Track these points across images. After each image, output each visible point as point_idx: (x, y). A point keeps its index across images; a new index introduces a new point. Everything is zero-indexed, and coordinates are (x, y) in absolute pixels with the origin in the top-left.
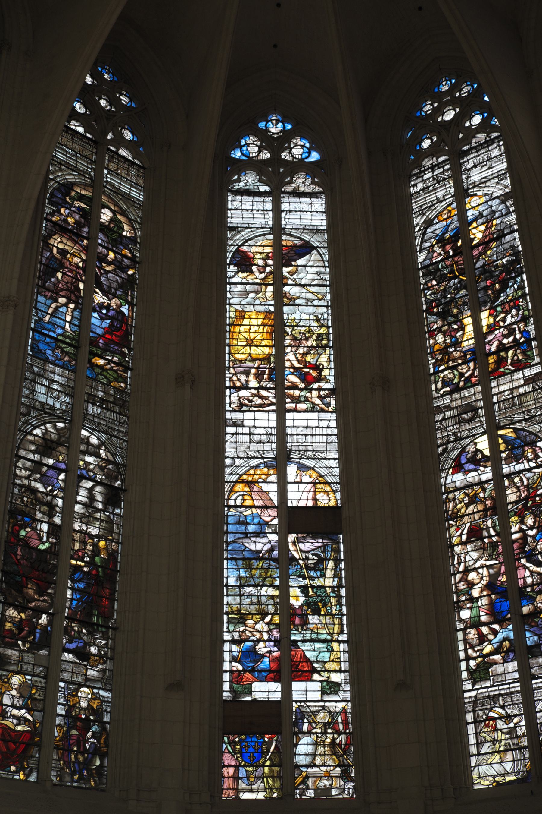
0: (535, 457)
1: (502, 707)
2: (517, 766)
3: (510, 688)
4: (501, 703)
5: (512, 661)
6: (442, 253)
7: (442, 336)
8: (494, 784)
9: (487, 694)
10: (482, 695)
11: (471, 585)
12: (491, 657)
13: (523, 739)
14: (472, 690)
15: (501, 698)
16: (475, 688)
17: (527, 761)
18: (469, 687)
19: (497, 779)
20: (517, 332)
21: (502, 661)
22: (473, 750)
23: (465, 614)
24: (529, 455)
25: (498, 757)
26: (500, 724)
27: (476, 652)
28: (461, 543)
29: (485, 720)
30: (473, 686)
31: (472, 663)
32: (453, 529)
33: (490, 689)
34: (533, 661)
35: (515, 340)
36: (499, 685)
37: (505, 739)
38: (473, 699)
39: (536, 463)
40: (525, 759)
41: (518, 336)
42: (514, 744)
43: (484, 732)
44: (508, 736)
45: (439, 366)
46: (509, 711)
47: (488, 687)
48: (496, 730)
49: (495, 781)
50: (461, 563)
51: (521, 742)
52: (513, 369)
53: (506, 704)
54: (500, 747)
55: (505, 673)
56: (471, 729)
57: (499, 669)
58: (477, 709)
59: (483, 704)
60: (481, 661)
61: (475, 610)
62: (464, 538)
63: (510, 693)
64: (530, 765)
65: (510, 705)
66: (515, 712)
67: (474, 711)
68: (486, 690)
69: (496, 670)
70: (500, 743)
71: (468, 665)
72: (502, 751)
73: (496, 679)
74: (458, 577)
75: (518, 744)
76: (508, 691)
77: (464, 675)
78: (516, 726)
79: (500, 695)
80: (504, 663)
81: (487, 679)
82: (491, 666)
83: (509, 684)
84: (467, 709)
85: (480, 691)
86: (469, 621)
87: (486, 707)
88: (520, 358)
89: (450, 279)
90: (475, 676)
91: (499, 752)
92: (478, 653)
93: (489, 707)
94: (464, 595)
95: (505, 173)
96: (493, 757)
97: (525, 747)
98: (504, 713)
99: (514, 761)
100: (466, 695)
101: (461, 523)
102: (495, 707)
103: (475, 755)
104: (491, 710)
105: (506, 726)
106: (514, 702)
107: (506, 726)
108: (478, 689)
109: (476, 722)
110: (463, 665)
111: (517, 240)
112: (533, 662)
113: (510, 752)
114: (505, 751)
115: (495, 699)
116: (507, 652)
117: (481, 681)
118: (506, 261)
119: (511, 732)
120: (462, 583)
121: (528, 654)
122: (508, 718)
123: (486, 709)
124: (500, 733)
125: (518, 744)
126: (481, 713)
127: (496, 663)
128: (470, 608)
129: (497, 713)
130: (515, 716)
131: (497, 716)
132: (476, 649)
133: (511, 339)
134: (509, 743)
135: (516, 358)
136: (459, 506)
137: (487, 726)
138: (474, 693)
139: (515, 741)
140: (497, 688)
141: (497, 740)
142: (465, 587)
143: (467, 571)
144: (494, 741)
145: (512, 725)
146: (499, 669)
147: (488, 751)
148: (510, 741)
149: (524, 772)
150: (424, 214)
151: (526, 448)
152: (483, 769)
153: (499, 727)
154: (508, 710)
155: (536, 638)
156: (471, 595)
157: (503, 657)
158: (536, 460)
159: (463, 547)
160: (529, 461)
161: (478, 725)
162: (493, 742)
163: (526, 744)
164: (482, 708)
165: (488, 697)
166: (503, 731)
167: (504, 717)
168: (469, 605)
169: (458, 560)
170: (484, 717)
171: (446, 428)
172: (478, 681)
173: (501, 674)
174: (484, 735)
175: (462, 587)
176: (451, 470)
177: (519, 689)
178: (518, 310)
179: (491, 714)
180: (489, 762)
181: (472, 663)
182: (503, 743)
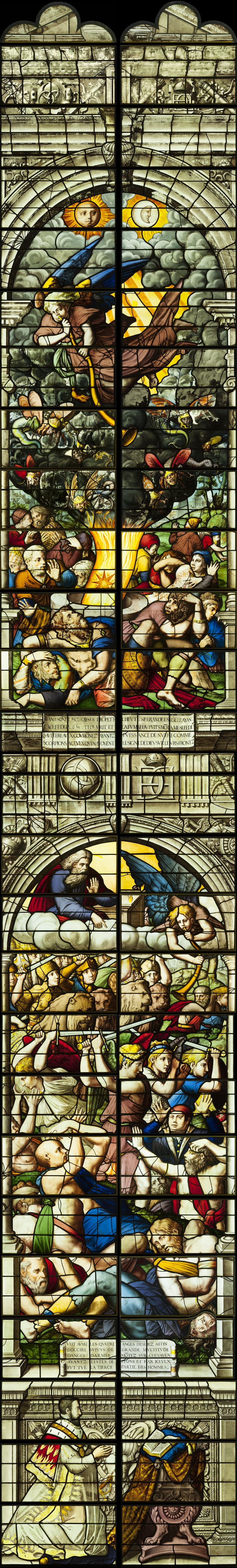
0: (191, 926)
6: (65, 323)
7: (39, 554)
8: (43, 1561)
9: (48, 1393)
10: (38, 1393)
11: (43, 1166)
14: (21, 1379)
20: (197, 617)
23: (24, 1225)
24: (181, 918)
28: (32, 1072)
29: (37, 1442)
30: (24, 1370)
32: (17, 1036)
35: (190, 629)
39: (192, 941)
41: (198, 628)
45: (26, 633)
48: (56, 1462)
49: (45, 1555)
50: (26, 1114)
52: (175, 702)
58: (27, 1416)
61: (45, 1220)
62: (40, 1062)
68: (48, 1384)
71: (17, 1331)
74: (19, 1142)
85: (35, 1384)
86: (29, 1239)
88: (195, 682)
89: (76, 409)
92: (42, 1309)
94: (25, 1185)
95: (228, 168)
101: (37, 1027)
104: (53, 1423)
108: (32, 1380)
111: (231, 373)
117: (40, 1365)
118: (198, 419)
120: (25, 1158)
123: (43, 1420)
128: (36, 1215)
132: (39, 1299)
133: (181, 628)
135: (185, 679)
136: (36, 989)
142: (30, 1167)
143: (37, 1136)
144: (53, 1482)
150: (32, 184)
151: (177, 901)
152: (29, 1532)
156: (40, 1188)
158: (193, 934)
159: (35, 1082)
160: (178, 932)
161: (24, 1448)
168: (33, 1208)
169: (21, 1107)
171: (26, 795)
175: (23, 1168)
176: (28, 899)
178: (207, 561)
180: (38, 1520)
181: (27, 1328)
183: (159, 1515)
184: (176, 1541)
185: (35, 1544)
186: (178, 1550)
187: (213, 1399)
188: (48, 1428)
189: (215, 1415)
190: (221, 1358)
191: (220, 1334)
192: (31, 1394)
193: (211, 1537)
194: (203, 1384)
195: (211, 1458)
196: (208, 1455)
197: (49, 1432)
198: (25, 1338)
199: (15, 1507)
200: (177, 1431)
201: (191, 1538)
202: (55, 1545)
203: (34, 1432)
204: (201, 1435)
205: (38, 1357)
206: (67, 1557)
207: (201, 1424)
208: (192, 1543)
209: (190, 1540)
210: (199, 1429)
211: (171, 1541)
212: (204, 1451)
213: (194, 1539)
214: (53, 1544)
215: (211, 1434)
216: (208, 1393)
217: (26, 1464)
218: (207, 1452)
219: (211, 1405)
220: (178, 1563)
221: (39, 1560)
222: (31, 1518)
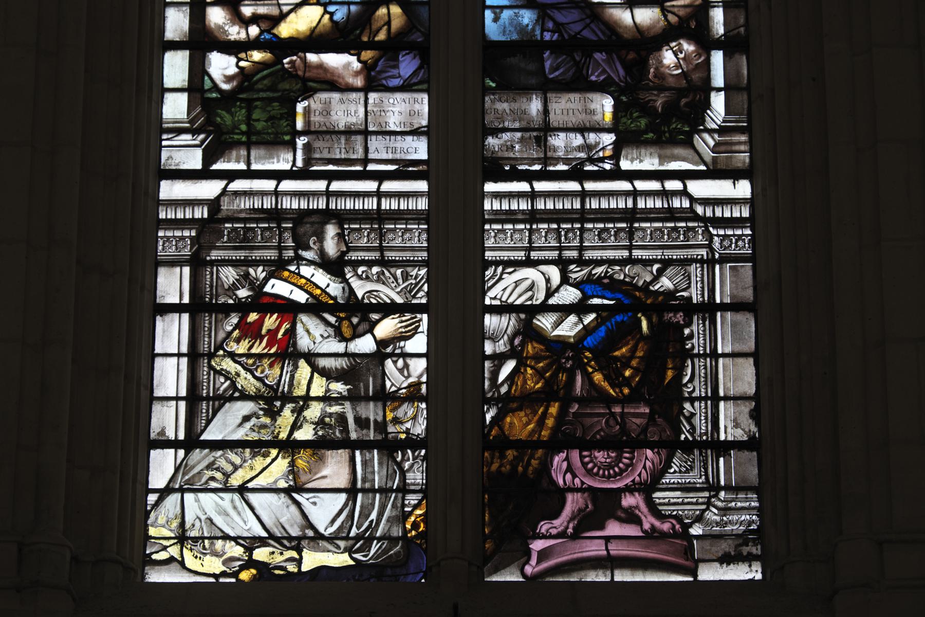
1: (335, 267)
2: (365, 515)
3: (379, 194)
4: (331, 247)
5: (406, 87)
8: (245, 576)
9: (268, 203)
10: (245, 204)
12: (312, 57)
13: (406, 410)
15: (331, 231)
16: (218, 166)
17: (412, 499)
18: (194, 160)
19: (261, 554)
21: (359, 82)
22: (168, 419)
25: (282, 465)
26: (312, 334)
27: (245, 22)
29: (242, 308)
30: (210, 156)
31: (221, 66)
33: (287, 185)
34: (504, 106)
36: (331, 177)
37: (326, 399)
38: (201, 213)
40: (404, 489)
42: (362, 423)
43: (232, 356)
44: (338, 387)
46: (360, 289)
47: (278, 176)
48: (288, 352)
49: (250, 563)
51: (396, 421)
53: (354, 256)
54: (295, 427)
55: (366, 133)
56: (171, 334)
57: (346, 111)
58: (215, 255)
59: (244, 240)
60: (262, 65)
63: (380, 217)
64: (426, 517)
65: (370, 264)
66: (389, 294)
67: (198, 263)
68: (269, 185)
69: (327, 112)
70: (299, 411)
72: (305, 444)
73: (322, 149)
75: (381, 427)
76: (371, 204)
77: (175, 107)
78: (386, 349)
79: (328, 215)
80: (366, 89)
81: (282, 139)
82: (307, 93)
83: (381, 177)
84: (164, 250)
85: (238, 185)
87: (257, 254)
90: (225, 118)
91: (289, 447)
92: (254, 30)
93: (271, 254)
96: (259, 462)
97: (412, 443)
98: (335, 289)
99: (352, 491)
100: (169, 190)
102: (298, 259)
103: (174, 444)
104: (277, 268)
105: (340, 347)
106: (390, 255)
107: (340, 347)
109: (198, 307)
110: (175, 69)
112: (499, 106)
113: (343, 454)
114: (320, 445)
115: (307, 228)
116: (392, 48)
117: (248, 146)
119: (361, 375)
121: (486, 73)
122: (354, 314)
123: (255, 263)
124: (304, 370)
125: (381, 427)
126: (229, 275)
127: (331, 83)
129: (308, 285)
130: (388, 309)
131: (300, 297)
132: (247, 11)
134: (341, 419)
137: (251, 332)
138: (210, 189)
139: (371, 411)
140: (321, 185)
141: (287, 398)
144: (272, 400)
145: (365, 345)
146: (346, 111)
147: (239, 435)
148: (347, 409)
149: (393, 540)
153: (303, 342)
154: (355, 283)
155: (527, 17)
157: (368, 68)
161: (207, 320)
162: (269, 401)
163: (419, 429)
164: (241, 254)
165: (276, 215)
166: (323, 363)
167: (334, 308)
170: (243, 293)
172: (238, 144)
173: (349, 132)
174: (229, 365)
177: (422, 204)
179: (278, 287)
180: (236, 480)
181: (221, 66)
182: (314, 411)
183: (570, 469)
184: (614, 528)
185: (226, 537)
186: (617, 549)
187: (696, 218)
188: (266, 280)
189: (703, 252)
190: (722, 130)
191: (718, 79)
192: (226, 205)
193: (699, 519)
194: (674, 185)
195: (697, 344)
196: (691, 336)
197: (268, 289)
198: (215, 87)
199: (181, 453)
200: (609, 285)
201: (649, 521)
202: (278, 540)
203: (234, 287)
204: (670, 294)
205: (244, 127)
206: (305, 568)
207: (670, 271)
208: (652, 536)
209: (647, 526)
210: (665, 283)
211: (602, 528)
212: (681, 328)
213: (657, 524)
214: (271, 536)
215: (695, 294)
216: (686, 204)
217: (211, 356)
218: (687, 331)
219: (693, 228)
220: (618, 578)
221: (235, 575)
222: (218, 475)
